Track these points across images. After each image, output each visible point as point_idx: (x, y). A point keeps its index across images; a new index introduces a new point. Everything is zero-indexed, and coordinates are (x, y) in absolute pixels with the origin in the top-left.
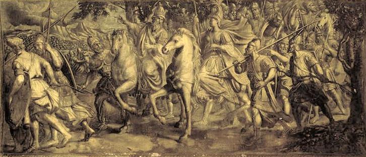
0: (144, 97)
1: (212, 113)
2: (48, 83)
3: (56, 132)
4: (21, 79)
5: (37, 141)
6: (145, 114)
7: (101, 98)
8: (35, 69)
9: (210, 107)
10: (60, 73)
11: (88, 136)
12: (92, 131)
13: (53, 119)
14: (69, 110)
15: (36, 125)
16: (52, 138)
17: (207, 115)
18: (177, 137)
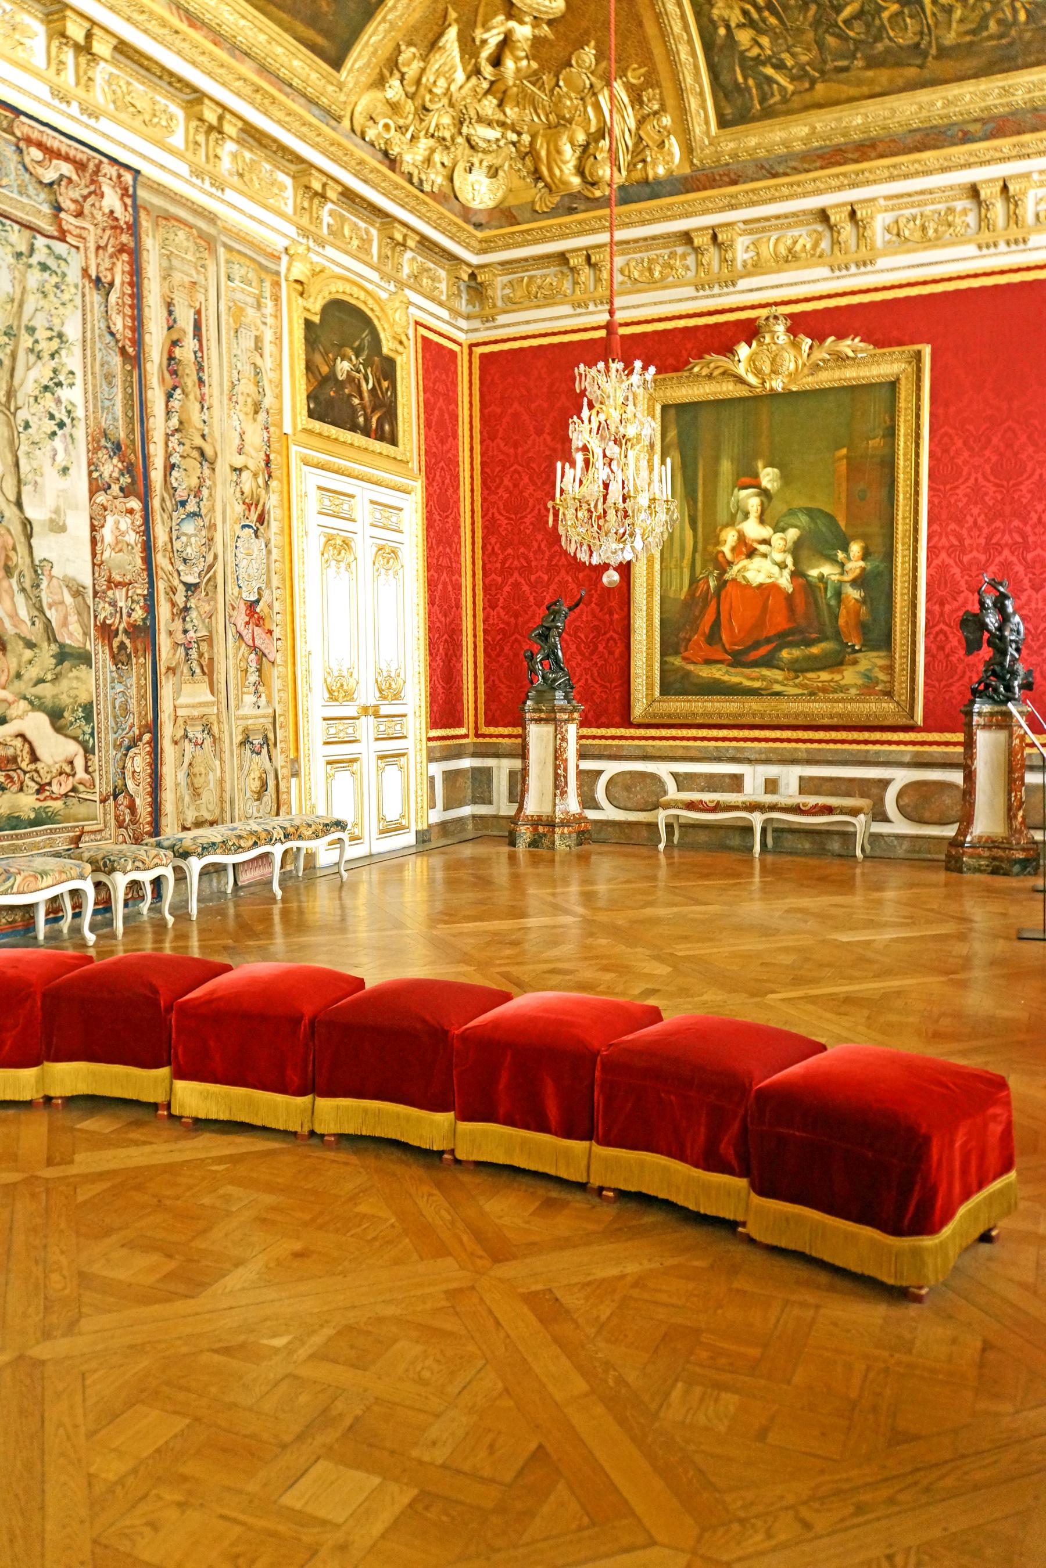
0: (873, 19)
1: (961, 21)
2: (754, 28)
3: (775, 86)
4: (722, 31)
5: (756, 102)
6: (878, 39)
7: (820, 31)
8: (735, 17)
9: (958, 14)
10: (766, 14)
11: (813, 82)
12: (817, 75)
13: (769, 71)
14: (785, 56)
15: (751, 82)
16: (773, 95)
17: (954, 25)
18: (918, 62)
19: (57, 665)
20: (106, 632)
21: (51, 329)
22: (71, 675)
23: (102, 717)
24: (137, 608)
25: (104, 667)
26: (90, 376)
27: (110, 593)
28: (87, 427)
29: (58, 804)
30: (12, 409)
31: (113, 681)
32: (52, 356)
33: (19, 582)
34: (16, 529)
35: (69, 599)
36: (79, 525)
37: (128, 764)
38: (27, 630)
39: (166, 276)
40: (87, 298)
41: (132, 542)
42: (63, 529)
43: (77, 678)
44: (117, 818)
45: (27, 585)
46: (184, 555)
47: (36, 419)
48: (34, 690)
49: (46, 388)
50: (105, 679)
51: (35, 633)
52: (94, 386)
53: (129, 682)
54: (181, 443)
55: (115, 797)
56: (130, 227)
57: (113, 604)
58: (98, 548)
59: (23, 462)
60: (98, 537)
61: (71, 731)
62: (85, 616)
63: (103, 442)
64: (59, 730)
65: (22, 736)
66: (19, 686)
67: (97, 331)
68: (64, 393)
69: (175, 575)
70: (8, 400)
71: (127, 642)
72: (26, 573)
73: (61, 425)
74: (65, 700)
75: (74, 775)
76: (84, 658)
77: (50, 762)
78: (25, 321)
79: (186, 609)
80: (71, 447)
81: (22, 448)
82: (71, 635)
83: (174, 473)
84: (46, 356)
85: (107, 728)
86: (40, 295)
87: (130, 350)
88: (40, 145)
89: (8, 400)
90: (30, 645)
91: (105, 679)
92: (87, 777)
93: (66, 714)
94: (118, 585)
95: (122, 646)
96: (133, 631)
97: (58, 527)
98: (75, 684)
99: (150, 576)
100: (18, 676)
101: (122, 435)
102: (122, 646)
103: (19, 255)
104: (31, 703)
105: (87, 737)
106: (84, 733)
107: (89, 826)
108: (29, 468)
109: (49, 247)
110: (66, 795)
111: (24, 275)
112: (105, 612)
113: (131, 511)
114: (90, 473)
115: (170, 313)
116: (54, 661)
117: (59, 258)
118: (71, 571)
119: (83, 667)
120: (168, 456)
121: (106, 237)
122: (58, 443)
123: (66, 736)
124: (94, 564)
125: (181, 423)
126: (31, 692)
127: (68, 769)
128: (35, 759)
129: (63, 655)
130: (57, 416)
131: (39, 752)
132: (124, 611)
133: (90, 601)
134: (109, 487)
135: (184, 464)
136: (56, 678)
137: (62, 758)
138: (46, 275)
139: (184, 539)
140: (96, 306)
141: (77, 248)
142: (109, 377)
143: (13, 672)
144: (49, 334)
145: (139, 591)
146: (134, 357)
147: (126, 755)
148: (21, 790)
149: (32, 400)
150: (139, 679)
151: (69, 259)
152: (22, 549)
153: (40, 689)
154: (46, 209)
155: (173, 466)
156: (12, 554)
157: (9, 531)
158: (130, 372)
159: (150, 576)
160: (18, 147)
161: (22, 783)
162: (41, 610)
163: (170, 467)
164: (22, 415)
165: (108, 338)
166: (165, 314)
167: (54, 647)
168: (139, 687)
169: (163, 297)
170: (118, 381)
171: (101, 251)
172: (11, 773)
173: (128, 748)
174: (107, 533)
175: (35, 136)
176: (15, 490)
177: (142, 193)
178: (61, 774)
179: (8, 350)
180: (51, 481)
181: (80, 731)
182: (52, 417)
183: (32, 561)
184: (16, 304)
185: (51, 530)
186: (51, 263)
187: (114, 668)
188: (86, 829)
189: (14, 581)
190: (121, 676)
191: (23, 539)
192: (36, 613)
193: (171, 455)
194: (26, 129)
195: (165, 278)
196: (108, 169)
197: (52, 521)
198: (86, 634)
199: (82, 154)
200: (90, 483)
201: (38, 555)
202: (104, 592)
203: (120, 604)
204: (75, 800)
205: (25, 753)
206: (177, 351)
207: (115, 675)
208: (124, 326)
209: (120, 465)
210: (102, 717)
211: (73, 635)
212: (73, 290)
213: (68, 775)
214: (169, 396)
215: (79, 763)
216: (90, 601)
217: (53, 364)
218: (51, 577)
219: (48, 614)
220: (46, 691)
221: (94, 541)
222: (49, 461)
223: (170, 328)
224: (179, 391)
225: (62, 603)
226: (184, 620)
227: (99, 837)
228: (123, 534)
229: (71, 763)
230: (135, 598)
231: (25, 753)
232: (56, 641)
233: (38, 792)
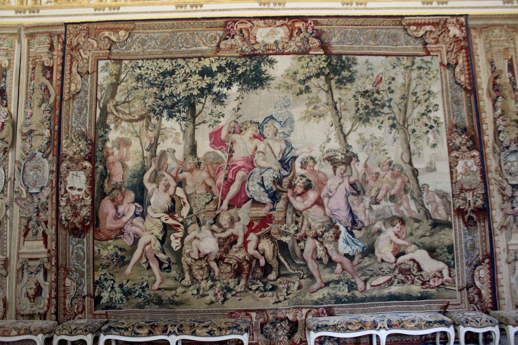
19: (432, 229)
20: (460, 212)
21: (425, 91)
22: (440, 233)
23: (459, 251)
24: (479, 200)
25: (460, 228)
26: (446, 104)
27: (462, 195)
28: (446, 125)
29: (434, 291)
30: (406, 126)
31: (465, 234)
32: (426, 101)
33: (411, 195)
34: (409, 173)
35: (438, 200)
36: (443, 167)
37: (476, 273)
38: (416, 215)
39: (488, 51)
40: (443, 74)
41: (475, 170)
42: (435, 170)
43: (443, 234)
44: (469, 299)
45: (416, 195)
46: (510, 171)
47: (418, 127)
48: (420, 240)
49: (423, 114)
50: (460, 234)
51: (421, 215)
52: (448, 107)
53: (475, 235)
54: (503, 120)
55: (468, 289)
56: (465, 38)
57: (465, 199)
58: (454, 176)
59: (412, 146)
60: (453, 171)
61: (442, 257)
62: (448, 206)
63: (455, 130)
64: (433, 257)
65: (413, 260)
66: (412, 239)
67: (449, 85)
68: (432, 115)
69: (505, 181)
70: (404, 123)
71: (474, 216)
72: (415, 191)
73: (431, 127)
74: (436, 243)
75: (442, 278)
76: (449, 225)
77: (429, 271)
78: (411, 91)
79: (513, 197)
80: (437, 135)
81: (411, 140)
82: (440, 215)
83: (501, 135)
84: (423, 101)
85: (462, 256)
86: (419, 79)
87: (469, 88)
88: (414, 24)
89: (404, 123)
90: (417, 221)
91: (460, 234)
92: (450, 279)
93: (437, 250)
94: (467, 191)
95: (470, 218)
96: (478, 211)
97: (431, 169)
98: (443, 236)
99: (485, 185)
100: (411, 234)
101: (467, 124)
102: (470, 218)
103: (407, 67)
104: (418, 246)
105: (450, 260)
106: (448, 259)
107: (452, 302)
108: (415, 148)
109: (422, 60)
110: (438, 287)
111: (410, 74)
112: (459, 203)
113: (474, 157)
114: (448, 144)
115: (492, 66)
116: (430, 227)
117: (427, 62)
118: (440, 187)
119: (447, 229)
120: (496, 127)
121: (452, 46)
122: (430, 135)
123: (438, 260)
124: (452, 183)
125: (503, 111)
126: (418, 241)
127: (439, 275)
128: (420, 269)
129: (437, 225)
130: (429, 124)
131: (423, 267)
132: (472, 202)
133: (451, 199)
134: (460, 148)
135: (507, 129)
136: (432, 235)
137: (436, 269)
138: (421, 71)
139: (509, 164)
140: (448, 75)
141: (437, 55)
142: (457, 102)
143: (408, 233)
144: (424, 93)
145: (480, 192)
146: (472, 90)
147: (475, 269)
148: (413, 283)
149: (416, 121)
150: (481, 233)
151: (432, 61)
152: (412, 181)
153: (423, 240)
154: (420, 46)
155: (500, 132)
156: (408, 184)
157: (406, 175)
158: (470, 97)
159: (485, 185)
160: (404, 29)
161: (413, 281)
162: (423, 206)
163: (497, 133)
164: (410, 128)
165: (456, 86)
166: (490, 67)
167: (430, 221)
168: (482, 237)
169: (488, 60)
170: (464, 102)
171: (449, 53)
172: (408, 276)
173: (476, 266)
174: (460, 168)
175: (412, 22)
176: (408, 158)
177: (471, 23)
178: (435, 277)
179: (403, 104)
180: (427, 152)
181: (445, 258)
182: (426, 125)
183: (418, 186)
184: (406, 86)
185: (428, 171)
186: (424, 65)
187: (466, 228)
188: (450, 303)
189: (409, 195)
190: (469, 232)
191: (413, 177)
192: (421, 207)
193: (498, 127)
194: (408, 21)
195: (488, 52)
196: (450, 20)
197: (428, 167)
198: (448, 214)
199: (436, 20)
200: (449, 149)
201: (421, 183)
202: (459, 195)
203: (469, 199)
204: (444, 289)
205: (415, 267)
206: (498, 81)
207: (466, 231)
208: (465, 79)
209: (466, 137)
210: (459, 251)
211: (441, 215)
212: (435, 72)
213: (439, 278)
214: (495, 101)
215: (445, 272)
216: (451, 199)
217: (426, 104)
218: (428, 191)
219: (427, 207)
220: (427, 240)
221: (451, 173)
222: (426, 143)
223: (492, 72)
224: (500, 98)
225: (435, 201)
226: (512, 202)
227: (458, 307)
228: (470, 167)
229: (441, 272)
230: (478, 195)
231: (415, 267)
232: (431, 218)
233: (422, 284)
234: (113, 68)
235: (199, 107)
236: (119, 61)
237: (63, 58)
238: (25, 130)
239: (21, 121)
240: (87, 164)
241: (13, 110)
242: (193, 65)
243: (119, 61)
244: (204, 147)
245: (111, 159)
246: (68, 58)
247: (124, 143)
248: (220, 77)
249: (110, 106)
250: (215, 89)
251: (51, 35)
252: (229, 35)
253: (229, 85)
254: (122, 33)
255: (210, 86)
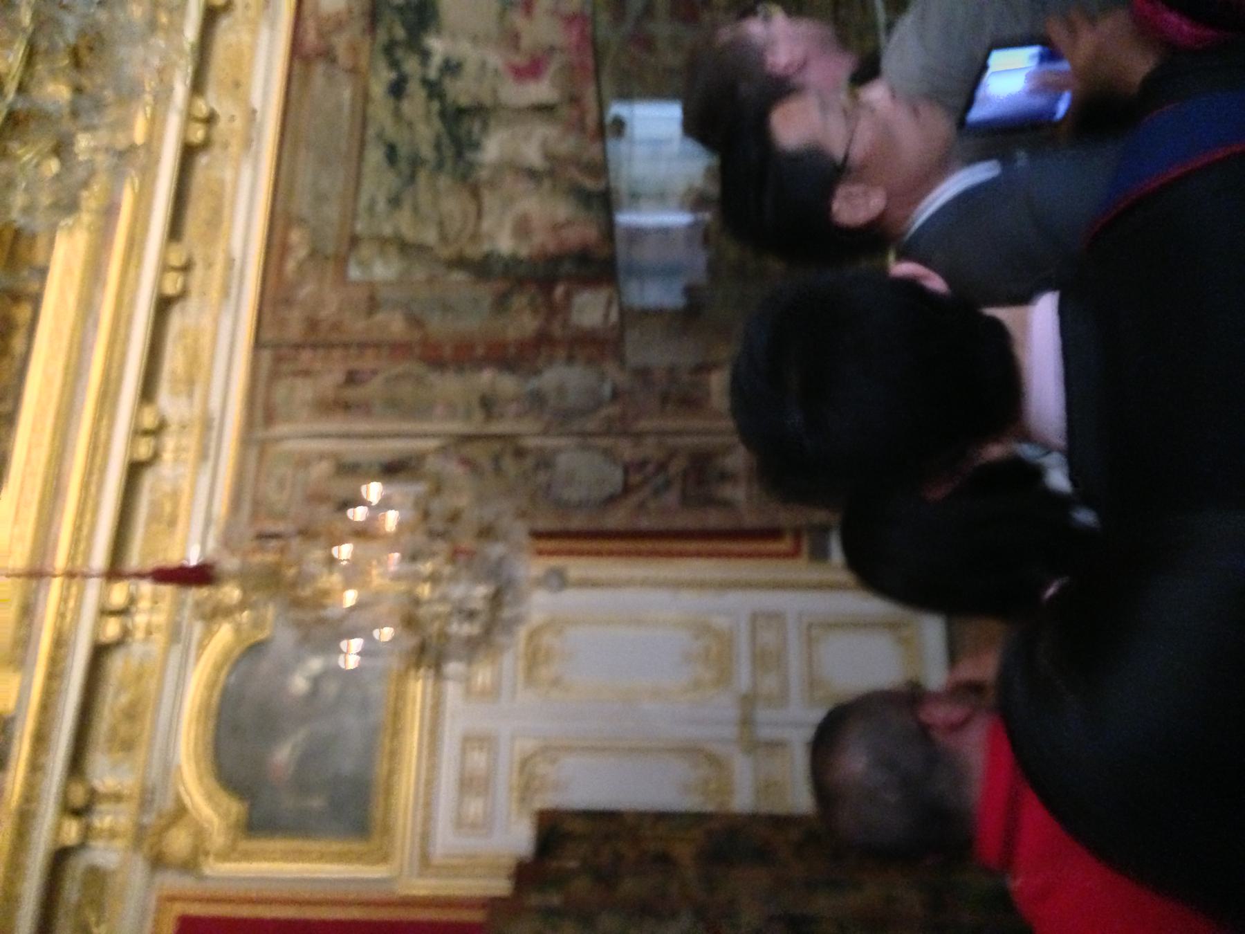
234: (366, 251)
235: (464, 101)
236: (354, 241)
237: (330, 346)
238: (478, 415)
239: (457, 427)
240: (559, 291)
241: (432, 444)
242: (381, 110)
243: (354, 241)
244: (542, 91)
245: (551, 247)
246: (334, 337)
247: (523, 228)
248: (411, 65)
249: (446, 252)
250: (433, 74)
251: (275, 376)
252: (328, 55)
253: (425, 55)
254: (295, 236)
255: (426, 82)
